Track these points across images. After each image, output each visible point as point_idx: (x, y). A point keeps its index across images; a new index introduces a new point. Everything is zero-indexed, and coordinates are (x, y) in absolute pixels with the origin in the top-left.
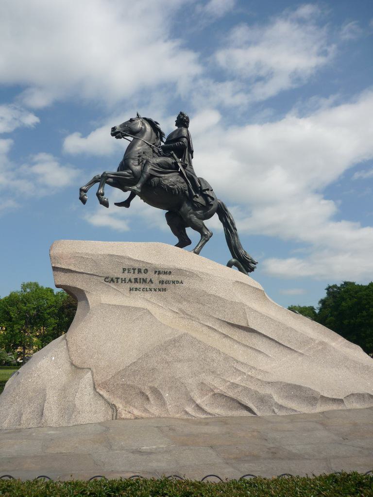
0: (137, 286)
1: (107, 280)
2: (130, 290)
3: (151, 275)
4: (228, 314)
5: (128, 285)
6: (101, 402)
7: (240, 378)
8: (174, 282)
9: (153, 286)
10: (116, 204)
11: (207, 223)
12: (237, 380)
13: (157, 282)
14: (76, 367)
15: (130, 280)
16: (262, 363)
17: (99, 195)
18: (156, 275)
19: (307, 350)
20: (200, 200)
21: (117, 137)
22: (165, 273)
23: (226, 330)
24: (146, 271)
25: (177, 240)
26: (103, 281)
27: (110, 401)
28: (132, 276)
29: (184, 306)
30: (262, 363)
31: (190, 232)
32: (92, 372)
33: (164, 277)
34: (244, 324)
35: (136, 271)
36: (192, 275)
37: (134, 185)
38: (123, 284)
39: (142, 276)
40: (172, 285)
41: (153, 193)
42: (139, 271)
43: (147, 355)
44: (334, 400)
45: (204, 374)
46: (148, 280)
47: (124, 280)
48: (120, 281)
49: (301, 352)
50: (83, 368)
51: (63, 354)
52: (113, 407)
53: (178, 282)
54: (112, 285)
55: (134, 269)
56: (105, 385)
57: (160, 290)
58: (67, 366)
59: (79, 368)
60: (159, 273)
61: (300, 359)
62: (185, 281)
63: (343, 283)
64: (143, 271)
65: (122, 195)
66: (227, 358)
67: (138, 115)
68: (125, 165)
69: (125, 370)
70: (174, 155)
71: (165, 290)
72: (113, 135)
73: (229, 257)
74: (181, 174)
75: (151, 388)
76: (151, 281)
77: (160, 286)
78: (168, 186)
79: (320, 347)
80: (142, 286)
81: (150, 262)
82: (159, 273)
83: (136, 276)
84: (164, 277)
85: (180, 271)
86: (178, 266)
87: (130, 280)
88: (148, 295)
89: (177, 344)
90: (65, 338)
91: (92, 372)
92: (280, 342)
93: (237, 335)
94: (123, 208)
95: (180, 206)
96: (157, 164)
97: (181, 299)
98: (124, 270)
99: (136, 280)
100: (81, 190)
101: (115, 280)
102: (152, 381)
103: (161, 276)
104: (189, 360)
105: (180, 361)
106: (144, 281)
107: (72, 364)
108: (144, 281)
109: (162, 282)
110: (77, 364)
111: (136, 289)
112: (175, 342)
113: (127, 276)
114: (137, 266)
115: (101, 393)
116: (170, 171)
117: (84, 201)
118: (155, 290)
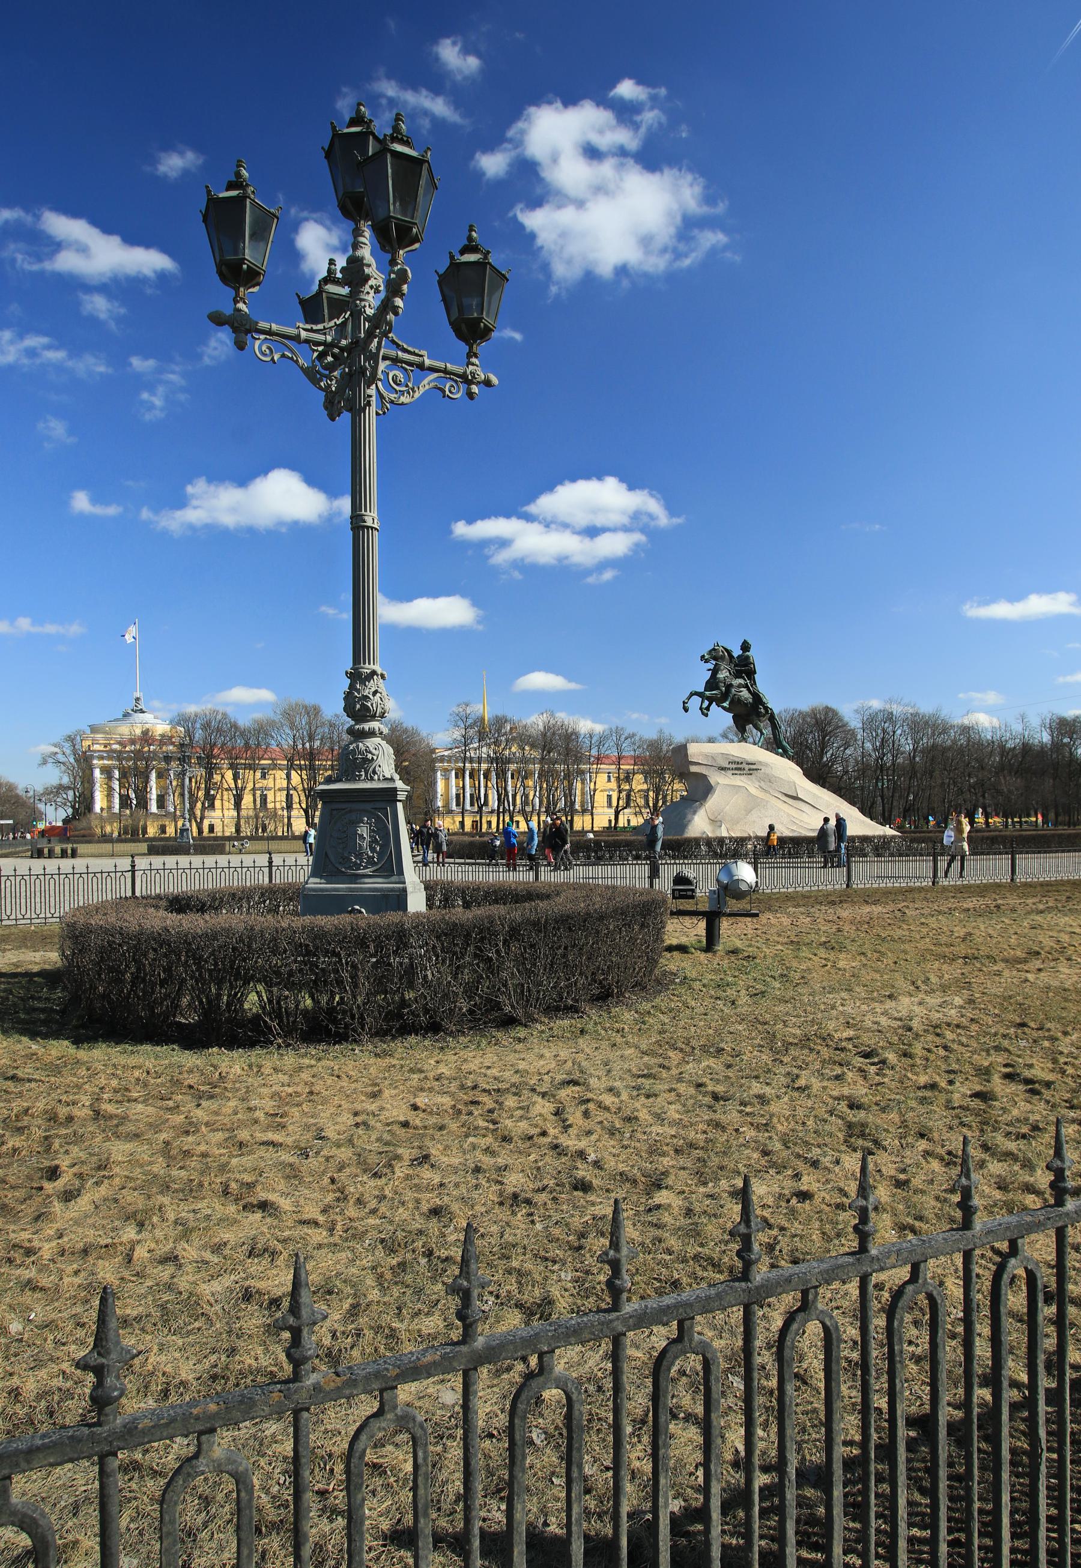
3: (744, 766)
12: (794, 828)
16: (804, 818)
28: (734, 766)
29: (762, 784)
30: (804, 818)
36: (766, 765)
62: (763, 768)
66: (788, 815)
88: (742, 777)
93: (790, 801)
97: (760, 780)
99: (736, 769)
106: (740, 769)
108: (740, 769)
113: (731, 766)
114: (737, 760)
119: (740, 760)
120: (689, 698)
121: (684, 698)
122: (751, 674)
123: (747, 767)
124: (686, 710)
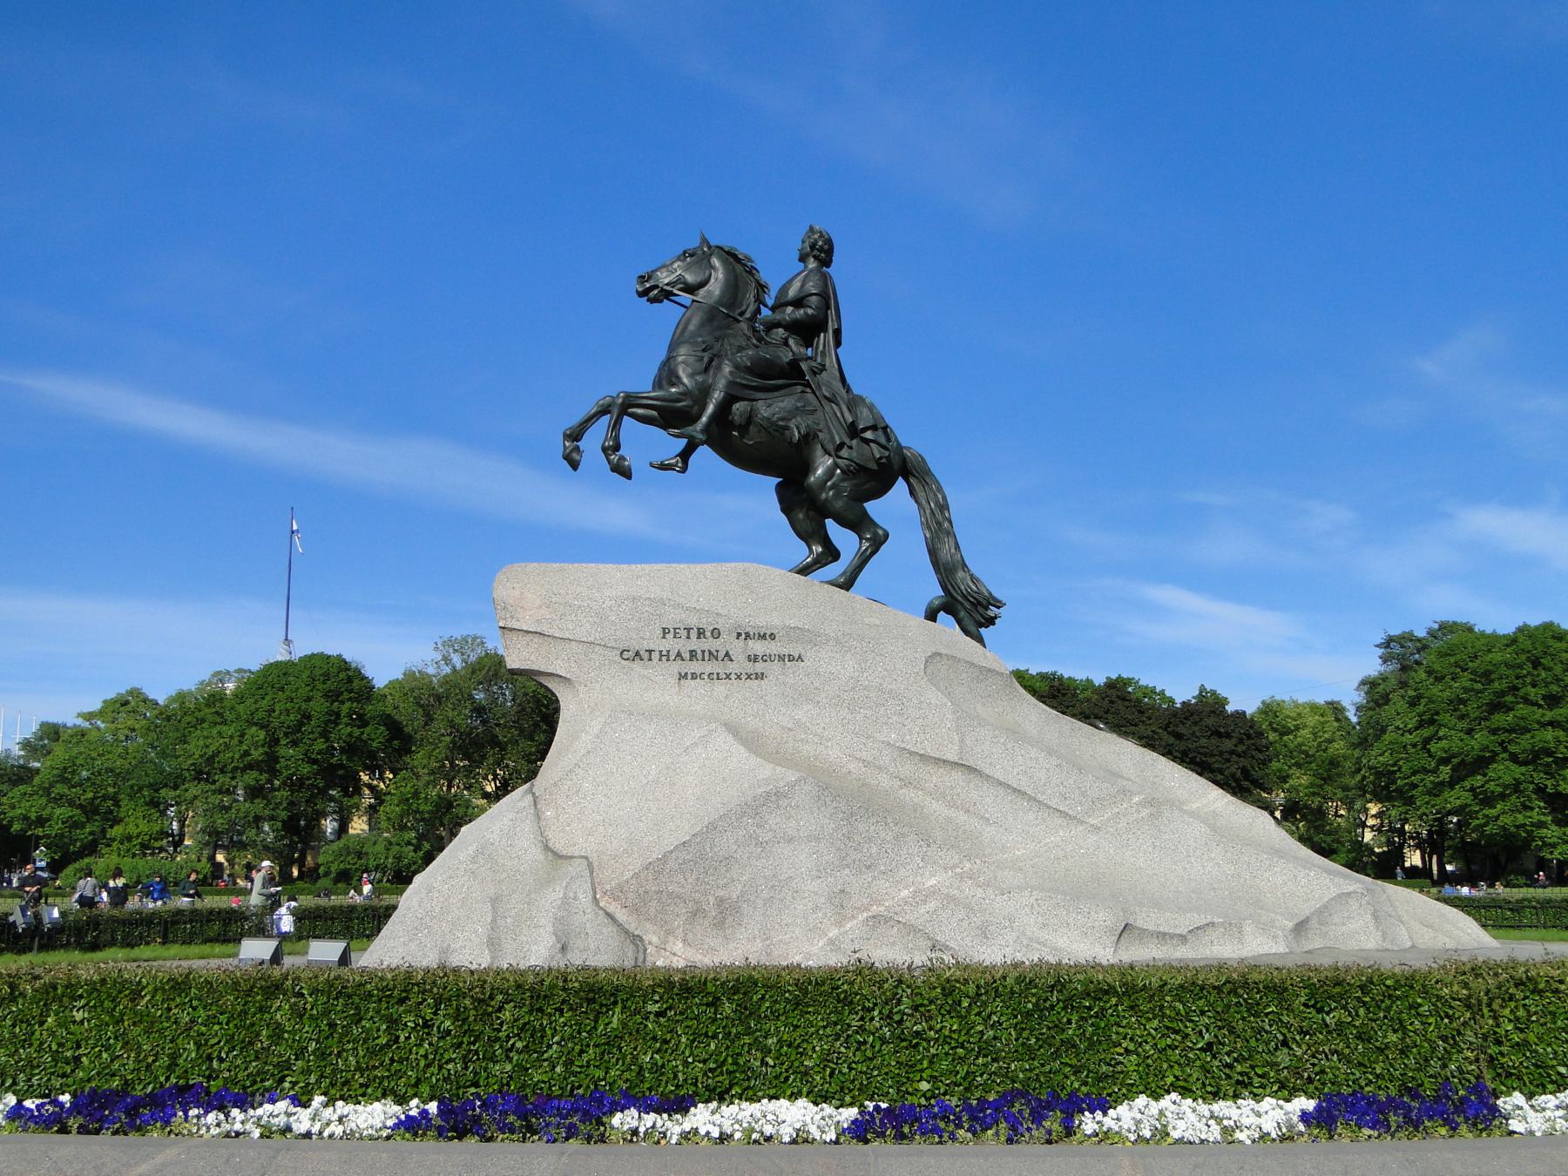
0: (695, 667)
1: (626, 655)
4: (910, 733)
5: (676, 667)
6: (610, 929)
7: (933, 882)
8: (781, 658)
9: (732, 668)
10: (652, 465)
11: (873, 508)
14: (555, 853)
15: (679, 654)
17: (612, 448)
18: (741, 642)
19: (1109, 820)
21: (652, 301)
22: (763, 637)
23: (907, 769)
24: (716, 633)
25: (801, 552)
26: (618, 658)
27: (632, 927)
31: (831, 525)
32: (590, 865)
33: (758, 647)
34: (951, 756)
35: (694, 634)
38: (664, 663)
39: (709, 644)
40: (776, 666)
41: (740, 444)
42: (701, 633)
43: (712, 827)
44: (1162, 936)
45: (847, 871)
46: (721, 654)
47: (665, 656)
48: (655, 656)
49: (1092, 821)
50: (572, 857)
51: (528, 826)
52: (636, 940)
53: (791, 658)
54: (637, 666)
55: (688, 630)
56: (618, 893)
57: (749, 677)
58: (536, 854)
59: (562, 857)
60: (747, 635)
61: (1093, 838)
62: (808, 656)
63: (1436, 626)
64: (708, 634)
65: (668, 444)
68: (667, 374)
69: (664, 859)
70: (791, 342)
71: (760, 676)
73: (935, 591)
75: (721, 901)
76: (727, 654)
77: (750, 668)
78: (774, 424)
79: (1145, 812)
80: (708, 667)
81: (725, 612)
83: (694, 644)
84: (758, 647)
85: (796, 633)
86: (792, 623)
87: (679, 654)
88: (720, 688)
89: (783, 802)
90: (530, 790)
91: (590, 865)
92: (1040, 797)
96: (747, 368)
98: (665, 631)
99: (693, 654)
100: (567, 437)
101: (646, 656)
102: (725, 885)
103: (750, 642)
104: (810, 838)
105: (790, 840)
106: (713, 656)
107: (547, 848)
108: (713, 656)
109: (753, 659)
110: (558, 844)
111: (694, 676)
112: (775, 797)
113: (670, 644)
114: (693, 621)
115: (611, 909)
116: (780, 382)
117: (575, 465)
118: (739, 677)
119: (707, 623)
123: (737, 648)
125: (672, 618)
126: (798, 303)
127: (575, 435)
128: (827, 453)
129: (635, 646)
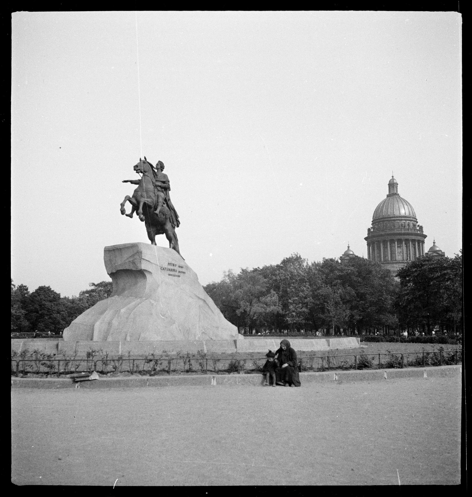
0: (171, 273)
2: (169, 275)
3: (176, 268)
13: (177, 272)
20: (175, 223)
33: (181, 270)
37: (156, 209)
60: (180, 267)
67: (145, 158)
71: (179, 276)
72: (135, 170)
74: (168, 205)
82: (180, 267)
84: (181, 270)
94: (129, 218)
95: (165, 224)
100: (121, 205)
106: (174, 270)
108: (174, 270)
109: (179, 272)
111: (171, 275)
114: (173, 263)
120: (125, 201)
121: (122, 201)
122: (166, 189)
124: (123, 212)
125: (170, 261)
126: (164, 182)
127: (122, 205)
128: (170, 222)
129: (164, 266)
